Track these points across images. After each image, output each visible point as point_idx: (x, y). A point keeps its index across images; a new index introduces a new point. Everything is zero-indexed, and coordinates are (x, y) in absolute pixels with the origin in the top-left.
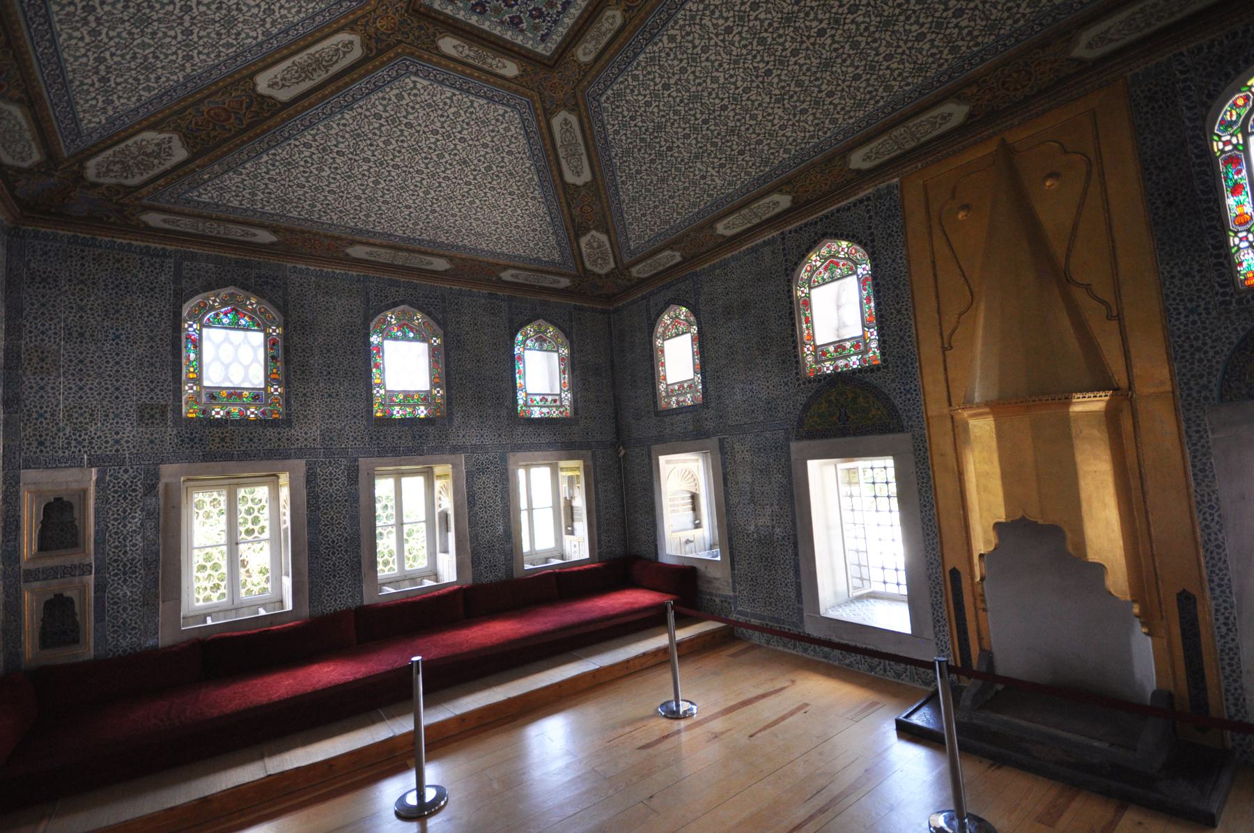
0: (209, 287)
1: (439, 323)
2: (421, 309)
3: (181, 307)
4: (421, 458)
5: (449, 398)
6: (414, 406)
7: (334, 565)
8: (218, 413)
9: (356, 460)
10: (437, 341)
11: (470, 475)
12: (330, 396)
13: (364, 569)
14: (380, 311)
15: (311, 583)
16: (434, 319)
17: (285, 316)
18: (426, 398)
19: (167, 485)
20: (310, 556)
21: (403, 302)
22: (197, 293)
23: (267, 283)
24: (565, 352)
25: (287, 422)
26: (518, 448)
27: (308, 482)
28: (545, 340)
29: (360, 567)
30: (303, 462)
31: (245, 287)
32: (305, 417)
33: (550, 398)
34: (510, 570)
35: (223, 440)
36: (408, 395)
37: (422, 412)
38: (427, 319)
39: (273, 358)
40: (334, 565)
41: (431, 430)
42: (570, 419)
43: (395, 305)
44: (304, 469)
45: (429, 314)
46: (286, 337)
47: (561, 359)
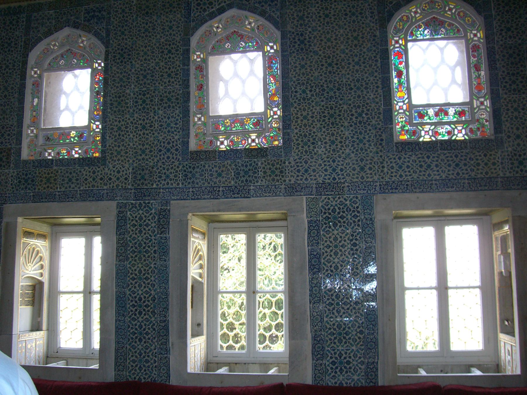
0: (49, 33)
1: (276, 24)
2: (253, 10)
3: (28, 55)
4: (245, 202)
5: (286, 121)
6: (245, 134)
7: (141, 327)
8: (50, 155)
9: (167, 203)
10: (271, 48)
11: (314, 227)
12: (144, 127)
13: (173, 338)
14: (203, 21)
15: (117, 342)
16: (270, 19)
17: (107, 47)
18: (259, 122)
19: (7, 224)
20: (118, 313)
21: (230, 6)
22: (40, 40)
23: (93, 17)
24: (478, 35)
25: (102, 160)
26: (389, 188)
27: (119, 227)
28: (442, 24)
29: (167, 335)
30: (114, 204)
31: (76, 26)
32: (119, 153)
33: (451, 111)
34: (372, 369)
35: (48, 180)
36: (236, 118)
37: (254, 141)
38: (262, 21)
39: (98, 93)
40: (141, 327)
41: (260, 162)
42: (489, 141)
43: (222, 11)
44: (115, 212)
45: (262, 14)
46: (106, 70)
47: (472, 50)
